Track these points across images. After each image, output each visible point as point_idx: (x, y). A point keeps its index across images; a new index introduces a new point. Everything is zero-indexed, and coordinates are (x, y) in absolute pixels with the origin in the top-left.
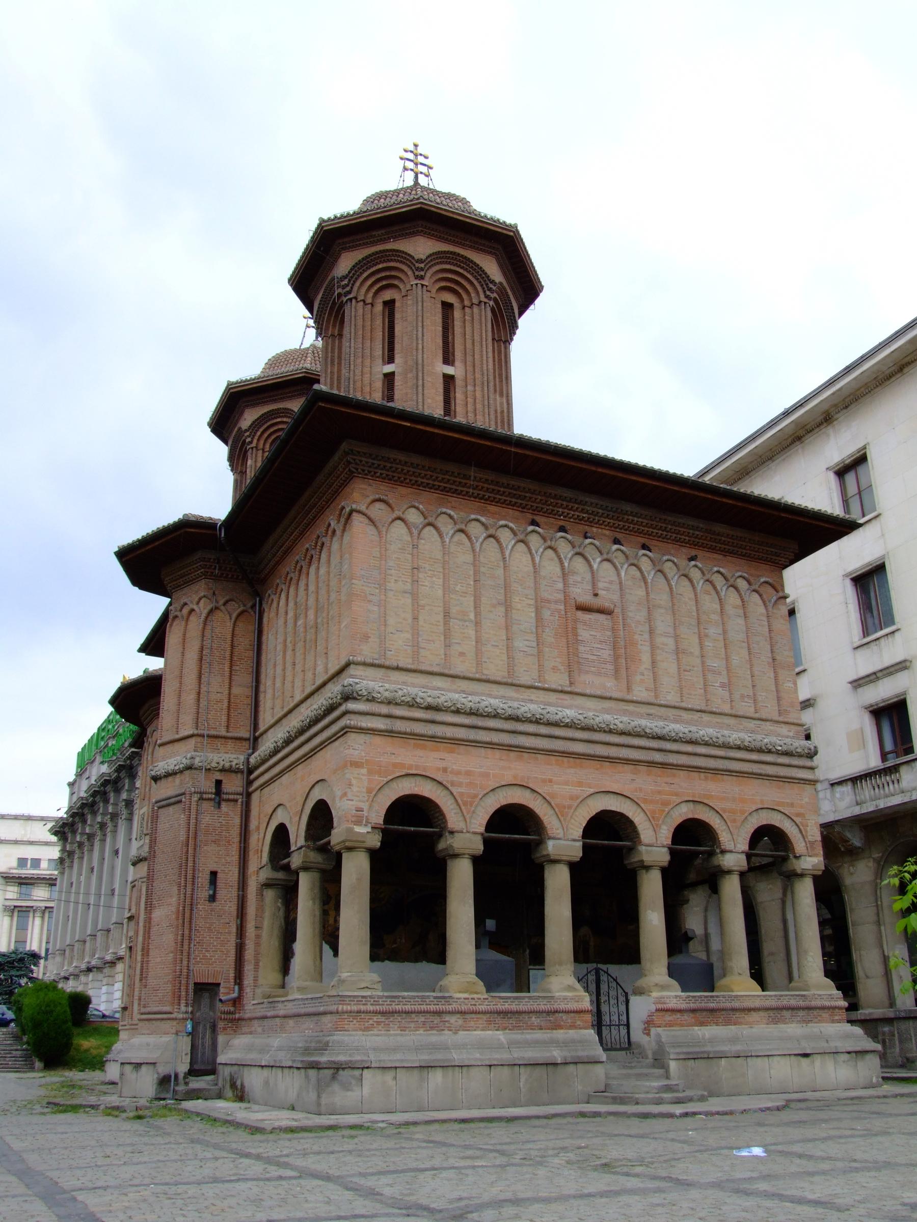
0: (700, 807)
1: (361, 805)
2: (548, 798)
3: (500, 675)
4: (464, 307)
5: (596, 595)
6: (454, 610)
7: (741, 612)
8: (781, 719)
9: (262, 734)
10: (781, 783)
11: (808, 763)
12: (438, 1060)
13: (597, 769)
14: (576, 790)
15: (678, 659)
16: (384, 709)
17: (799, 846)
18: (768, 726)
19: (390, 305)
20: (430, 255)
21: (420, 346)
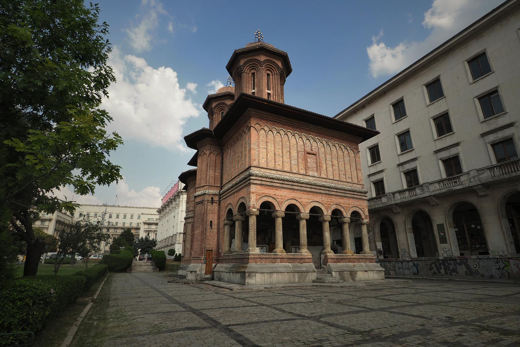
0: (338, 206)
4: (273, 75)
5: (312, 150)
6: (276, 153)
8: (358, 183)
9: (224, 185)
11: (365, 195)
12: (275, 271)
14: (308, 201)
15: (332, 167)
16: (260, 179)
17: (363, 217)
18: (355, 185)
19: (253, 74)
20: (265, 60)
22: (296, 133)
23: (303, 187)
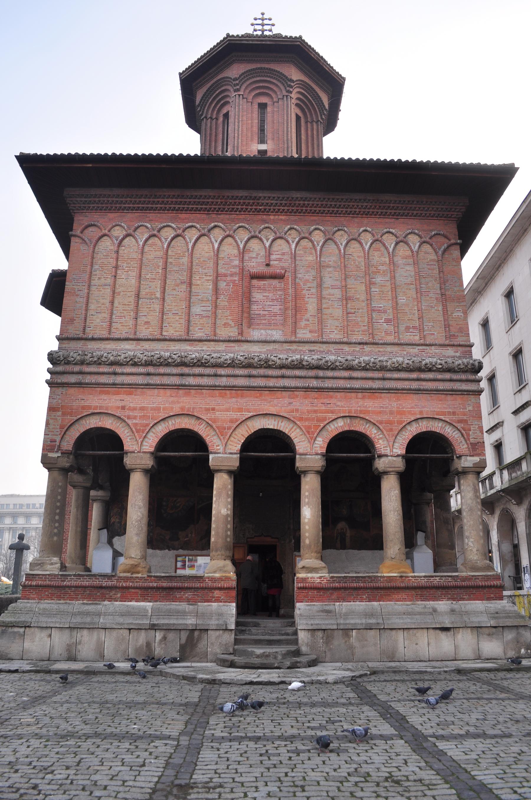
0: (357, 421)
1: (54, 437)
2: (210, 422)
3: (176, 335)
6: (143, 293)
7: (411, 261)
8: (447, 342)
10: (443, 396)
12: (85, 623)
13: (257, 397)
19: (226, 116)
20: (243, 74)
21: (236, 135)
22: (215, 226)
23: (221, 376)
